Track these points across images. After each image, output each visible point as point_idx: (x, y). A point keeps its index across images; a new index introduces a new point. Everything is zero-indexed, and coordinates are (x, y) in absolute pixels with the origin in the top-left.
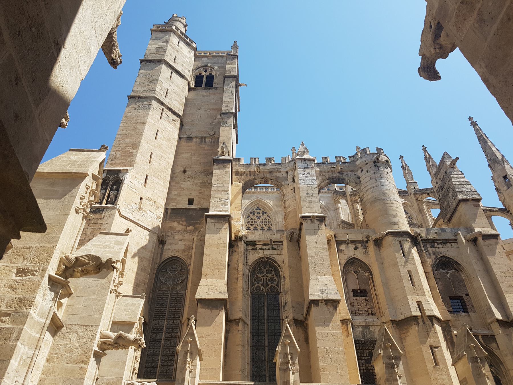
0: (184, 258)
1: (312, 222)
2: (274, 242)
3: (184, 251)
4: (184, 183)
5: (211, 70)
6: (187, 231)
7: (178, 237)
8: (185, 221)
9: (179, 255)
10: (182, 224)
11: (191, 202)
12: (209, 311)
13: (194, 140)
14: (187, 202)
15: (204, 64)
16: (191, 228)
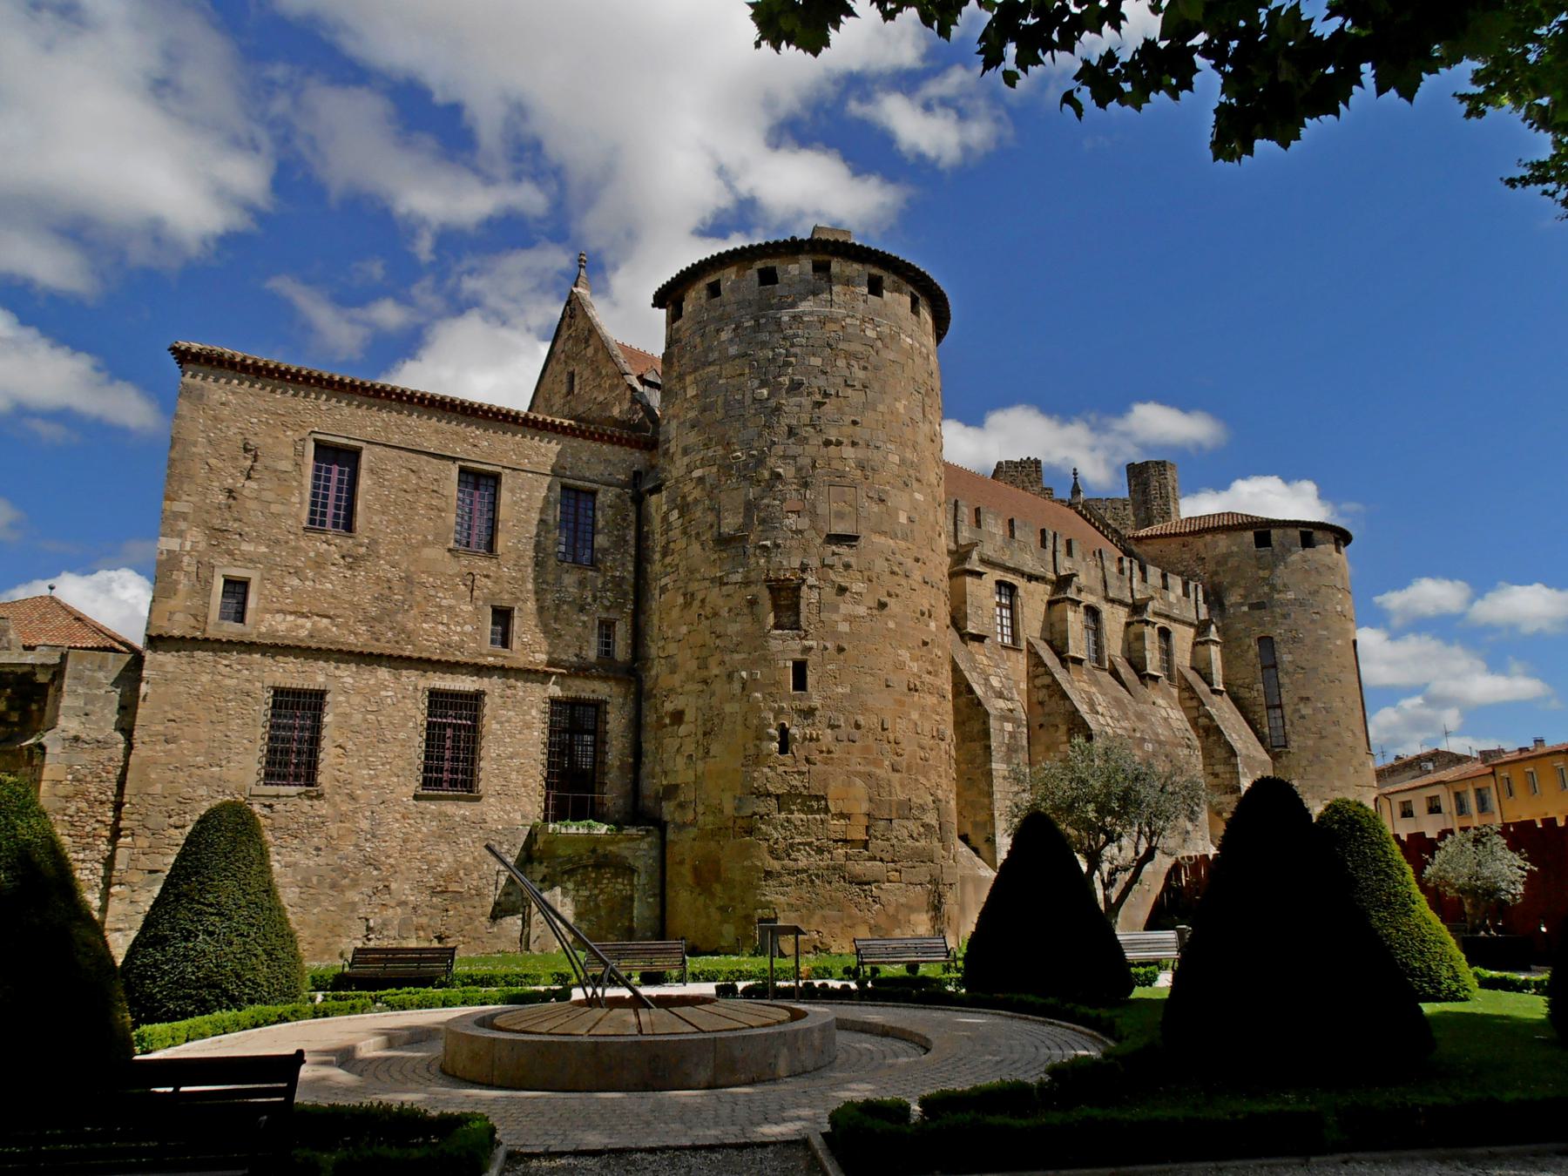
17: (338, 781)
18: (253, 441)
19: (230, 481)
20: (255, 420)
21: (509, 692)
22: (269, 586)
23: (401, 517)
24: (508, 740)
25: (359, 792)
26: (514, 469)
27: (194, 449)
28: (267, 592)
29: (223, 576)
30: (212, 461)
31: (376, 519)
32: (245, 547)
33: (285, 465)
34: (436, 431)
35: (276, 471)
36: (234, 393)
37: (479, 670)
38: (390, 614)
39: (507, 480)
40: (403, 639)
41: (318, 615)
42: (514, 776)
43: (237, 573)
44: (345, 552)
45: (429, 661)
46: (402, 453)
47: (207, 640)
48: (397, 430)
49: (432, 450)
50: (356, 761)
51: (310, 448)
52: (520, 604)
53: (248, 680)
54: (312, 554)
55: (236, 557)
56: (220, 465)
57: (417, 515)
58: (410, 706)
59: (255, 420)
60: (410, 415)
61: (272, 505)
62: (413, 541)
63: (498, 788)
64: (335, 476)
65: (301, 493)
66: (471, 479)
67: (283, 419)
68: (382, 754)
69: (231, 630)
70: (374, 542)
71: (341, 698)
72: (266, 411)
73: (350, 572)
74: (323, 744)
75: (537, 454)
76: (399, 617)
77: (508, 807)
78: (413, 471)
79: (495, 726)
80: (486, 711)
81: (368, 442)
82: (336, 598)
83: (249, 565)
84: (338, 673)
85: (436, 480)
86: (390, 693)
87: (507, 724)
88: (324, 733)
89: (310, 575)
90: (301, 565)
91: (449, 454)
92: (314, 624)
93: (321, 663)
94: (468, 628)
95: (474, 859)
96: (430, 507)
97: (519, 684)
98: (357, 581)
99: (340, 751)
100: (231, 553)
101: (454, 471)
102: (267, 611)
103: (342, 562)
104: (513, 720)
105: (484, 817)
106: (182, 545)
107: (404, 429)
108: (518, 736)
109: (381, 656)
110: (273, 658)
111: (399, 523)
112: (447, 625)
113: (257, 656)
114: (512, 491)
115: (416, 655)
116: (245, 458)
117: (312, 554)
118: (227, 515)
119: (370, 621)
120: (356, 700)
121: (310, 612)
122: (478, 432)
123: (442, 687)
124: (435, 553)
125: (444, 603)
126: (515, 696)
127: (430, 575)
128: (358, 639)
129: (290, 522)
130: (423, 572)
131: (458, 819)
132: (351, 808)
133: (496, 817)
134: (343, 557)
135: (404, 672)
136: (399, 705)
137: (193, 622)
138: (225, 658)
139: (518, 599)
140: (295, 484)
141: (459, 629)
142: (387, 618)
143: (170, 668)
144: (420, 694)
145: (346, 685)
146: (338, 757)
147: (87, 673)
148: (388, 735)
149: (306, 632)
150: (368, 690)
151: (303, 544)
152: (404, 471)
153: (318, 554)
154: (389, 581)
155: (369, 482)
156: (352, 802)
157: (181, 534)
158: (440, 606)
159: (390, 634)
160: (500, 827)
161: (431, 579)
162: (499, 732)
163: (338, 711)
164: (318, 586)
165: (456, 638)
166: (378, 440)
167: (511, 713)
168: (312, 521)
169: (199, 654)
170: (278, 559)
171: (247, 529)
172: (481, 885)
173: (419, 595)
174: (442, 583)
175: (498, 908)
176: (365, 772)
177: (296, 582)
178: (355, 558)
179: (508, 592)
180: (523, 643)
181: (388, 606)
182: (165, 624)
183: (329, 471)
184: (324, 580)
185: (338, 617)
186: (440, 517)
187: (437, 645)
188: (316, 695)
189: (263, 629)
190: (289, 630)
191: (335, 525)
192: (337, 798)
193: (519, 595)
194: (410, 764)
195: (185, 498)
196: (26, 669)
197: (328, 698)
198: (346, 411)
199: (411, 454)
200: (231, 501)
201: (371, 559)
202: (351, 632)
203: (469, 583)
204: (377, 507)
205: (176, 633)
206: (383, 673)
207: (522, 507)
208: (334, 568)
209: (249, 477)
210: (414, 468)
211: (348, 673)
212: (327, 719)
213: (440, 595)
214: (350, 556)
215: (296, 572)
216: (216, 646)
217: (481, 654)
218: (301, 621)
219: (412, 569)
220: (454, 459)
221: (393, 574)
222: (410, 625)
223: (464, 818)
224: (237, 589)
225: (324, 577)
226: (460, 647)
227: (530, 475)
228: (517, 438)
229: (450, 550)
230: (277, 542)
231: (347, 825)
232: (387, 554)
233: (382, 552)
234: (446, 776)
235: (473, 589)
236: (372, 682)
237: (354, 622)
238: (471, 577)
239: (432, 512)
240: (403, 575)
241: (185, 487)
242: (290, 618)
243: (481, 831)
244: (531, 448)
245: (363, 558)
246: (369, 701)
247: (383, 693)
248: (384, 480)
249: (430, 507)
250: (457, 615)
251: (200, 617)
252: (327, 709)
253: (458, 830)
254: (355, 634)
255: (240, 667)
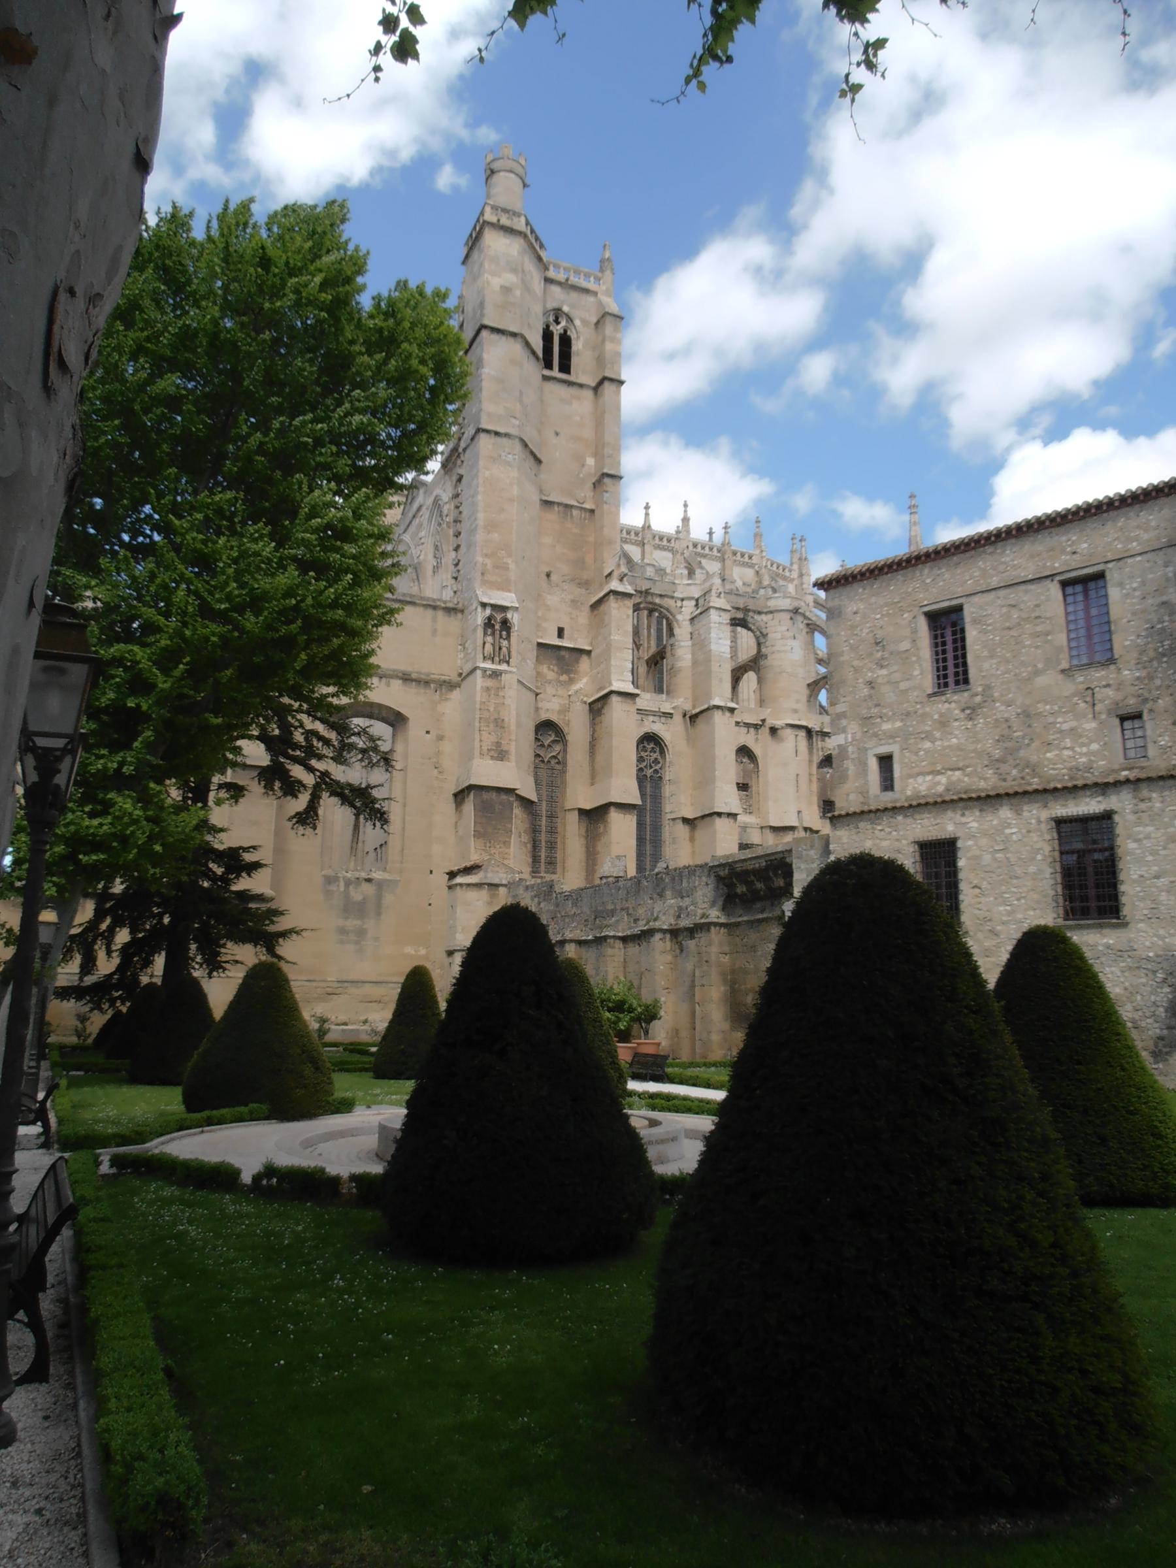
0: (561, 724)
1: (724, 714)
2: (664, 713)
3: (559, 712)
4: (549, 597)
5: (567, 321)
6: (560, 682)
7: (550, 690)
8: (556, 665)
9: (554, 718)
10: (553, 671)
11: (561, 633)
12: (622, 815)
13: (556, 508)
14: (556, 633)
15: (555, 305)
16: (564, 677)
17: (978, 919)
18: (880, 634)
19: (870, 674)
20: (878, 616)
21: (1143, 806)
22: (907, 754)
23: (1008, 655)
24: (1150, 858)
25: (999, 928)
26: (1119, 559)
27: (842, 659)
28: (907, 760)
29: (875, 755)
30: (855, 663)
31: (986, 665)
32: (886, 726)
33: (905, 645)
34: (1032, 556)
35: (899, 653)
36: (861, 600)
37: (1103, 788)
38: (1011, 752)
39: (1113, 576)
40: (1028, 774)
41: (951, 770)
42: (1163, 897)
43: (883, 750)
44: (964, 706)
45: (1045, 791)
46: (1002, 593)
47: (870, 811)
48: (994, 572)
49: (1030, 577)
50: (992, 899)
51: (923, 625)
52: (1149, 705)
53: (897, 840)
54: (936, 717)
55: (880, 737)
56: (861, 664)
57: (1024, 647)
58: (1035, 839)
59: (878, 616)
60: (1003, 552)
61: (901, 684)
62: (1024, 674)
63: (1146, 912)
64: (949, 639)
65: (920, 666)
66: (1079, 588)
67: (900, 605)
68: (1015, 890)
69: (887, 799)
70: (987, 688)
71: (970, 843)
72: (886, 605)
73: (970, 723)
74: (963, 886)
75: (1146, 530)
76: (1022, 753)
77: (1162, 932)
78: (1014, 606)
79: (1132, 845)
80: (1119, 830)
81: (967, 596)
82: (961, 750)
83: (891, 741)
84: (964, 820)
85: (1037, 606)
86: (1014, 830)
87: (1145, 842)
88: (961, 875)
89: (937, 734)
90: (928, 728)
91: (1049, 573)
92: (948, 778)
93: (950, 814)
94: (1095, 746)
95: (1126, 989)
96: (1036, 635)
97: (1154, 795)
98: (978, 729)
99: (977, 891)
100: (876, 735)
101: (1054, 590)
102: (910, 776)
103: (962, 716)
104: (1153, 835)
105: (1131, 944)
106: (846, 739)
107: (1002, 568)
108: (1161, 852)
109: (998, 796)
110: (912, 816)
111: (1008, 661)
112: (1072, 749)
113: (900, 818)
114: (1121, 585)
115: (1040, 788)
116: (878, 651)
117: (936, 717)
118: (870, 704)
119: (995, 763)
120: (984, 842)
121: (943, 769)
122: (1074, 538)
123: (1065, 815)
124: (1049, 680)
125: (1065, 727)
126: (1151, 808)
127: (1046, 703)
128: (987, 782)
129: (915, 694)
130: (1038, 702)
131: (1101, 948)
132: (994, 943)
133: (1147, 943)
134: (963, 710)
135: (1026, 808)
136: (1025, 840)
137: (861, 799)
138: (879, 824)
139: (1146, 700)
140: (914, 659)
141: (1084, 750)
142: (1010, 757)
143: (845, 840)
144: (1044, 827)
145: (972, 830)
146: (977, 896)
147: (804, 852)
148: (1018, 871)
149: (943, 787)
150: (993, 831)
151: (927, 709)
152: (1005, 610)
153: (941, 715)
154: (1007, 720)
155: (974, 633)
156: (995, 937)
157: (844, 730)
158: (1061, 731)
159: (1014, 772)
160: (1151, 954)
161: (1048, 707)
162: (1138, 851)
163: (969, 855)
164: (946, 744)
165: (1084, 760)
166: (979, 589)
167: (1150, 829)
168: (939, 688)
169: (862, 825)
170: (911, 729)
171: (884, 711)
172: (1137, 1018)
173: (1037, 725)
174: (1059, 707)
175: (1161, 1043)
176: (1001, 908)
177: (928, 745)
178: (973, 709)
179: (1133, 696)
180: (1161, 747)
181: (1008, 744)
182: (844, 804)
183: (943, 636)
184: (949, 737)
185: (968, 767)
186: (1047, 642)
187: (1065, 771)
188: (948, 843)
189: (909, 793)
190: (929, 789)
191: (957, 683)
192: (980, 936)
193: (1146, 695)
194: (1045, 896)
195: (843, 700)
196: (778, 857)
197: (959, 844)
198: (947, 576)
199: (1008, 591)
200: (872, 691)
201: (986, 704)
202: (981, 778)
203: (1088, 699)
204: (986, 653)
205: (852, 810)
206: (1005, 812)
207: (1134, 597)
208: (956, 724)
209: (882, 667)
210: (1013, 603)
211: (971, 818)
212: (961, 863)
213: (1059, 720)
214: (968, 708)
215: (926, 737)
216: (872, 815)
217: (1113, 771)
218: (939, 778)
219: (1028, 702)
220: (1051, 577)
221: (1011, 712)
222: (1034, 759)
223: (1108, 947)
224: (886, 761)
225: (951, 734)
226: (1089, 768)
227: (1139, 558)
228: (1120, 524)
229: (1063, 671)
230: (908, 714)
231: (993, 959)
232: (1002, 695)
233: (996, 695)
234: (1093, 904)
235: (1094, 705)
236: (995, 822)
237: (982, 768)
238: (1090, 692)
239: (1038, 639)
240: (1019, 711)
241: (841, 691)
242: (929, 778)
243: (1129, 960)
244: (1138, 527)
245: (980, 705)
246: (996, 840)
247: (1008, 831)
248: (988, 625)
249: (1036, 635)
250: (1081, 736)
251: (863, 792)
252: (960, 854)
253: (1103, 959)
254: (985, 779)
255: (890, 830)
